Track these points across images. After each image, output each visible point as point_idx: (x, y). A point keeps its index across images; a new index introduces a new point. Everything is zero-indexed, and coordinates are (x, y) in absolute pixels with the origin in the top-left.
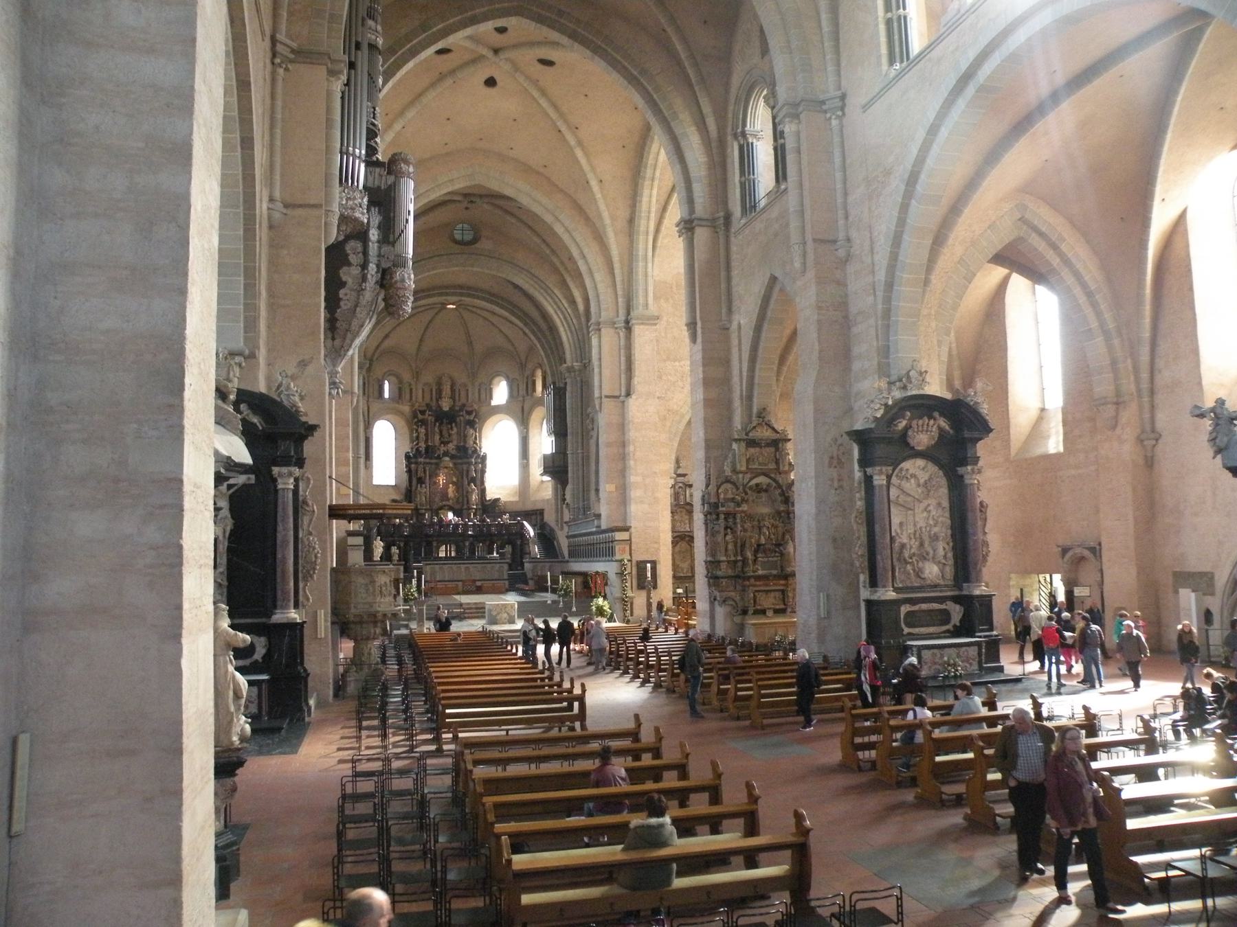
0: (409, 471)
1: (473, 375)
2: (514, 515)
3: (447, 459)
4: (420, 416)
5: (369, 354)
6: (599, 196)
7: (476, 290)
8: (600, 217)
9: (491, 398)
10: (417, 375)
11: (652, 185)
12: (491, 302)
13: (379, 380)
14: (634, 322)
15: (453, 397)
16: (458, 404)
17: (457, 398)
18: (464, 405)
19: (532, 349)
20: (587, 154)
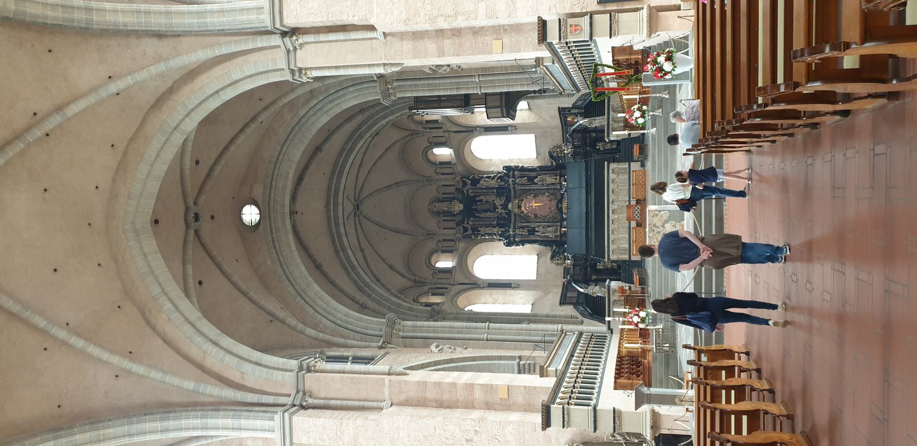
0: (523, 243)
1: (429, 180)
2: (565, 140)
3: (510, 206)
4: (470, 232)
5: (410, 283)
6: (129, 80)
7: (329, 189)
8: (161, 75)
9: (449, 163)
10: (430, 235)
11: (98, 10)
12: (341, 173)
13: (435, 272)
14: (278, 25)
15: (451, 200)
16: (456, 195)
17: (451, 195)
18: (457, 189)
19: (395, 125)
20: (74, 100)
